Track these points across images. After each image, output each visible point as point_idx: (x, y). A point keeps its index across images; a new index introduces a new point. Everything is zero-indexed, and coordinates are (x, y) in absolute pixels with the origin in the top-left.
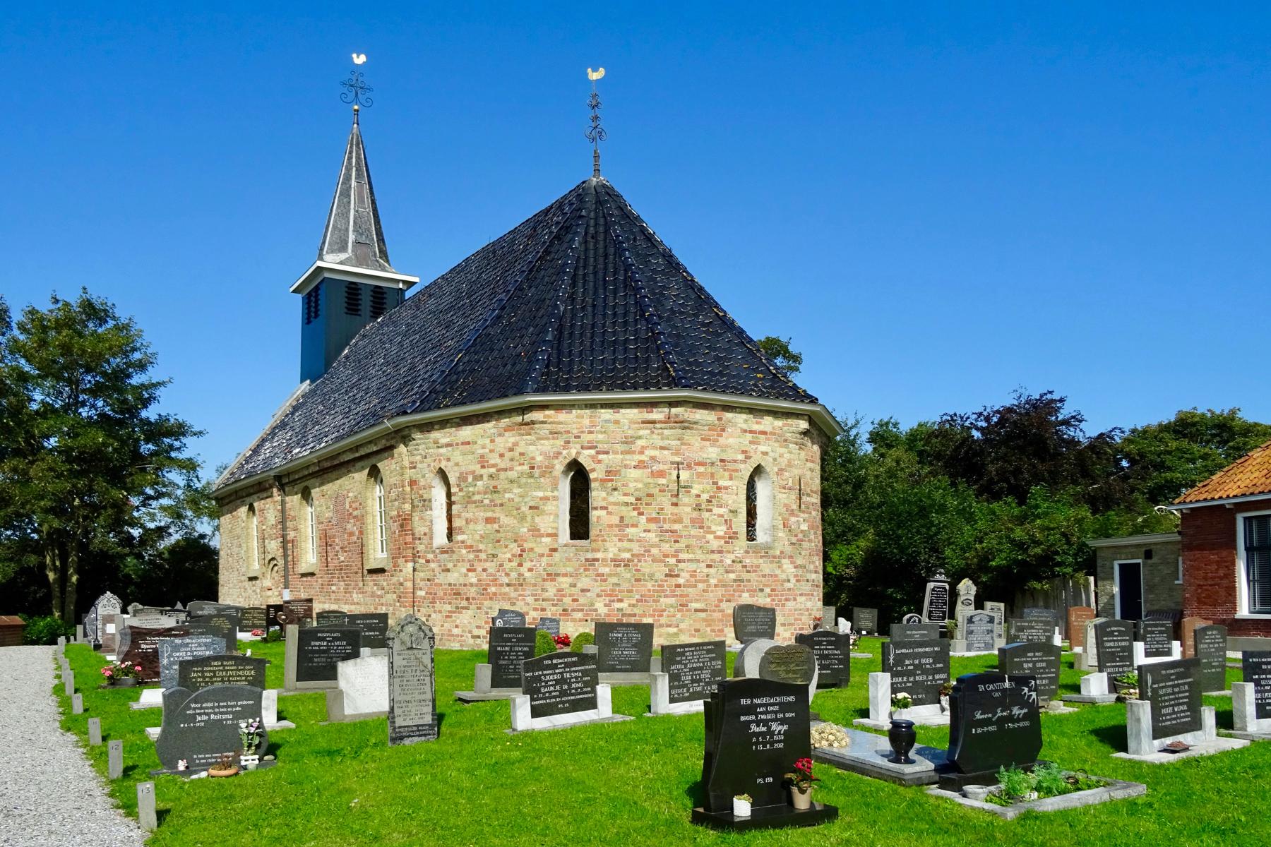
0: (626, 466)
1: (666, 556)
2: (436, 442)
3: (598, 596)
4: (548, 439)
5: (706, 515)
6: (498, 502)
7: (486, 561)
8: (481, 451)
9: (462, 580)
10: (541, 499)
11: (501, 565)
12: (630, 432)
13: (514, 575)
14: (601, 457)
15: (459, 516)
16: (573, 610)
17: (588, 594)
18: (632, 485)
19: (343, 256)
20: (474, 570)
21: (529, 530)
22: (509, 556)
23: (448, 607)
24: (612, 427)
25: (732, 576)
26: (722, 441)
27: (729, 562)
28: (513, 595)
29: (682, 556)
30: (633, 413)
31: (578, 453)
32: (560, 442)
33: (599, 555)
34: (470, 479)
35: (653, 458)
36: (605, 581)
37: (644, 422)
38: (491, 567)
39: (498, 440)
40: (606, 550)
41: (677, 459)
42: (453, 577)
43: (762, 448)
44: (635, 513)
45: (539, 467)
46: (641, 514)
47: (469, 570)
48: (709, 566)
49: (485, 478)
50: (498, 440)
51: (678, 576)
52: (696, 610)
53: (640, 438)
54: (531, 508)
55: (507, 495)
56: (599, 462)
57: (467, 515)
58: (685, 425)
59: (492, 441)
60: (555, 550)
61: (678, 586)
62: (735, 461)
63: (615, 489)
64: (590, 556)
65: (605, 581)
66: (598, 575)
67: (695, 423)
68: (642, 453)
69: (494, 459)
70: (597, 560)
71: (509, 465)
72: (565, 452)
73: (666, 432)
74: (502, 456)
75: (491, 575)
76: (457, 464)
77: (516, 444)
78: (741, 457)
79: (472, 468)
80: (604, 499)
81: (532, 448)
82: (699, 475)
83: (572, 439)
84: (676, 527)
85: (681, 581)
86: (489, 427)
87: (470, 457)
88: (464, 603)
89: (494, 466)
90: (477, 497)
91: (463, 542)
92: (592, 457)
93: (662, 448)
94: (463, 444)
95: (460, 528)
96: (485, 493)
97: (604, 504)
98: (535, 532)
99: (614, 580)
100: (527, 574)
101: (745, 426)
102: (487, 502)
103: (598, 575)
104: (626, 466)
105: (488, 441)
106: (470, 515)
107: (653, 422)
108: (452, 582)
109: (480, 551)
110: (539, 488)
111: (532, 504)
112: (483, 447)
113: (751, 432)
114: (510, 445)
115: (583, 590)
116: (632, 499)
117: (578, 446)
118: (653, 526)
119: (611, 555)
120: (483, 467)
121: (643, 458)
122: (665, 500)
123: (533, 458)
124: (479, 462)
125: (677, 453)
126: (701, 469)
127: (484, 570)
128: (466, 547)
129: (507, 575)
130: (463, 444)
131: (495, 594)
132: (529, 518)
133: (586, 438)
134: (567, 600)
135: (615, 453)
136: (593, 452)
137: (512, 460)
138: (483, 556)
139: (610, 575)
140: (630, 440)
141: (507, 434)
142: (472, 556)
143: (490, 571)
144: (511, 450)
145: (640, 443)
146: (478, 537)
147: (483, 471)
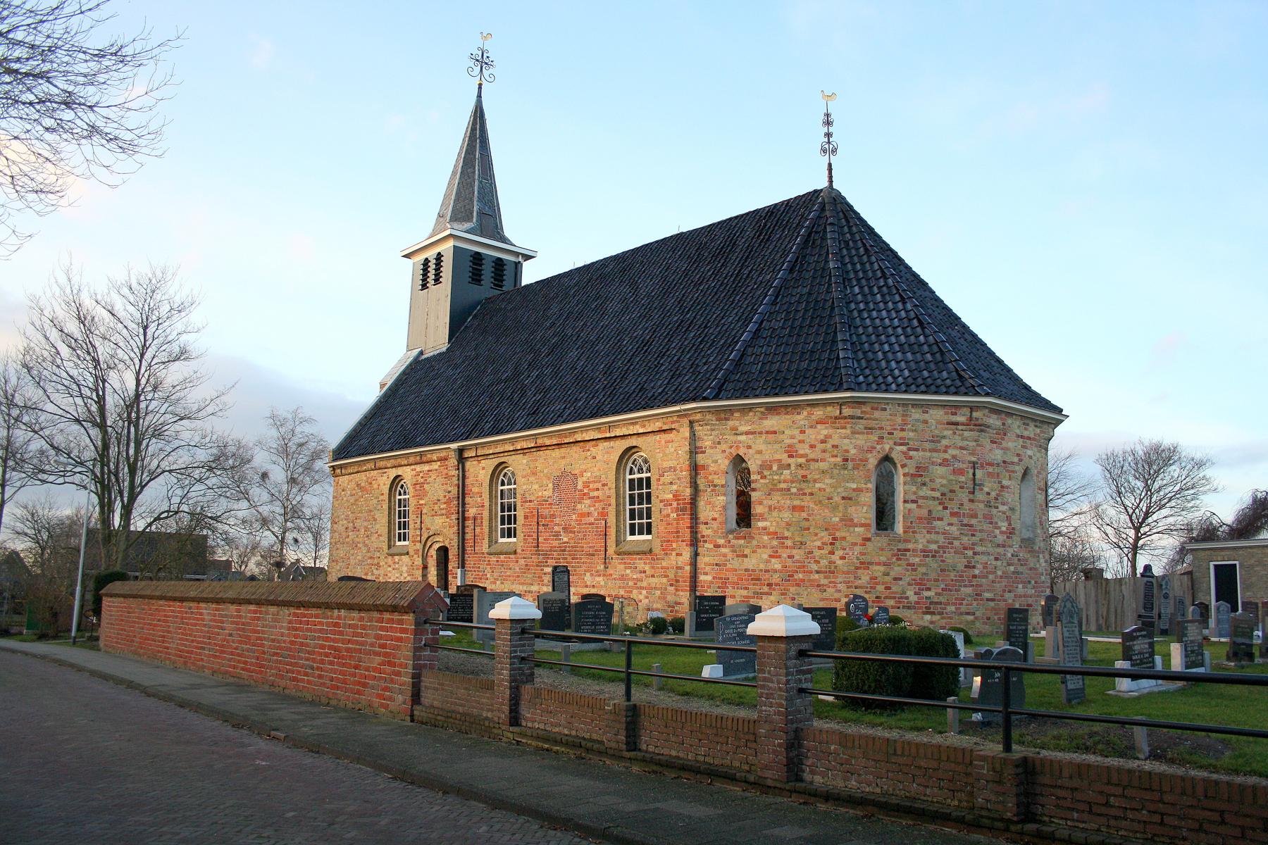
0: (933, 463)
1: (965, 548)
3: (909, 584)
5: (994, 511)
6: (808, 491)
8: (788, 441)
9: (762, 566)
10: (854, 490)
12: (937, 432)
13: (824, 562)
14: (911, 453)
15: (761, 503)
16: (886, 597)
18: (938, 481)
19: (468, 225)
20: (779, 557)
21: (841, 520)
22: (818, 543)
23: (745, 593)
24: (921, 426)
25: (1012, 568)
26: (1004, 444)
27: (1009, 555)
28: (824, 581)
29: (978, 549)
30: (937, 415)
31: (891, 449)
32: (874, 438)
33: (910, 546)
34: (775, 468)
35: (954, 457)
36: (915, 570)
37: (948, 423)
38: (798, 554)
40: (916, 542)
41: (974, 459)
42: (751, 563)
43: (1029, 452)
44: (940, 508)
45: (853, 460)
46: (945, 508)
48: (996, 559)
49: (793, 468)
51: (974, 567)
52: (988, 600)
53: (944, 437)
54: (843, 498)
55: (818, 485)
56: (911, 458)
57: (770, 502)
58: (982, 428)
59: (803, 432)
60: (869, 539)
61: (974, 576)
62: (1013, 463)
63: (924, 484)
64: (901, 546)
65: (915, 570)
66: (909, 565)
68: (945, 451)
70: (908, 550)
71: (820, 457)
73: (966, 434)
74: (812, 447)
75: (798, 561)
76: (760, 452)
77: (828, 436)
78: (1016, 459)
79: (777, 457)
80: (915, 493)
81: (846, 441)
82: (989, 474)
84: (973, 521)
85: (977, 572)
86: (801, 418)
87: (776, 446)
88: (766, 589)
89: (802, 456)
90: (783, 486)
91: (765, 528)
92: (904, 453)
93: (962, 448)
94: (767, 432)
95: (761, 515)
96: (792, 482)
97: (914, 498)
98: (848, 522)
99: (923, 570)
100: (839, 562)
101: (1018, 431)
102: (794, 490)
103: (909, 565)
104: (933, 463)
105: (797, 432)
107: (957, 424)
108: (751, 567)
109: (787, 538)
112: (792, 437)
113: (1022, 437)
114: (822, 437)
115: (895, 579)
116: (937, 494)
117: (891, 442)
118: (955, 520)
119: (920, 546)
121: (947, 456)
122: (964, 496)
123: (847, 451)
124: (786, 452)
125: (972, 454)
126: (991, 470)
127: (790, 557)
128: (769, 534)
130: (767, 432)
131: (803, 580)
132: (841, 508)
133: (898, 434)
134: (880, 588)
135: (924, 450)
136: (904, 448)
137: (824, 451)
138: (789, 543)
139: (920, 565)
140: (936, 440)
141: (819, 426)
142: (775, 543)
143: (797, 557)
144: (823, 442)
145: (944, 442)
146: (784, 525)
147: (791, 461)
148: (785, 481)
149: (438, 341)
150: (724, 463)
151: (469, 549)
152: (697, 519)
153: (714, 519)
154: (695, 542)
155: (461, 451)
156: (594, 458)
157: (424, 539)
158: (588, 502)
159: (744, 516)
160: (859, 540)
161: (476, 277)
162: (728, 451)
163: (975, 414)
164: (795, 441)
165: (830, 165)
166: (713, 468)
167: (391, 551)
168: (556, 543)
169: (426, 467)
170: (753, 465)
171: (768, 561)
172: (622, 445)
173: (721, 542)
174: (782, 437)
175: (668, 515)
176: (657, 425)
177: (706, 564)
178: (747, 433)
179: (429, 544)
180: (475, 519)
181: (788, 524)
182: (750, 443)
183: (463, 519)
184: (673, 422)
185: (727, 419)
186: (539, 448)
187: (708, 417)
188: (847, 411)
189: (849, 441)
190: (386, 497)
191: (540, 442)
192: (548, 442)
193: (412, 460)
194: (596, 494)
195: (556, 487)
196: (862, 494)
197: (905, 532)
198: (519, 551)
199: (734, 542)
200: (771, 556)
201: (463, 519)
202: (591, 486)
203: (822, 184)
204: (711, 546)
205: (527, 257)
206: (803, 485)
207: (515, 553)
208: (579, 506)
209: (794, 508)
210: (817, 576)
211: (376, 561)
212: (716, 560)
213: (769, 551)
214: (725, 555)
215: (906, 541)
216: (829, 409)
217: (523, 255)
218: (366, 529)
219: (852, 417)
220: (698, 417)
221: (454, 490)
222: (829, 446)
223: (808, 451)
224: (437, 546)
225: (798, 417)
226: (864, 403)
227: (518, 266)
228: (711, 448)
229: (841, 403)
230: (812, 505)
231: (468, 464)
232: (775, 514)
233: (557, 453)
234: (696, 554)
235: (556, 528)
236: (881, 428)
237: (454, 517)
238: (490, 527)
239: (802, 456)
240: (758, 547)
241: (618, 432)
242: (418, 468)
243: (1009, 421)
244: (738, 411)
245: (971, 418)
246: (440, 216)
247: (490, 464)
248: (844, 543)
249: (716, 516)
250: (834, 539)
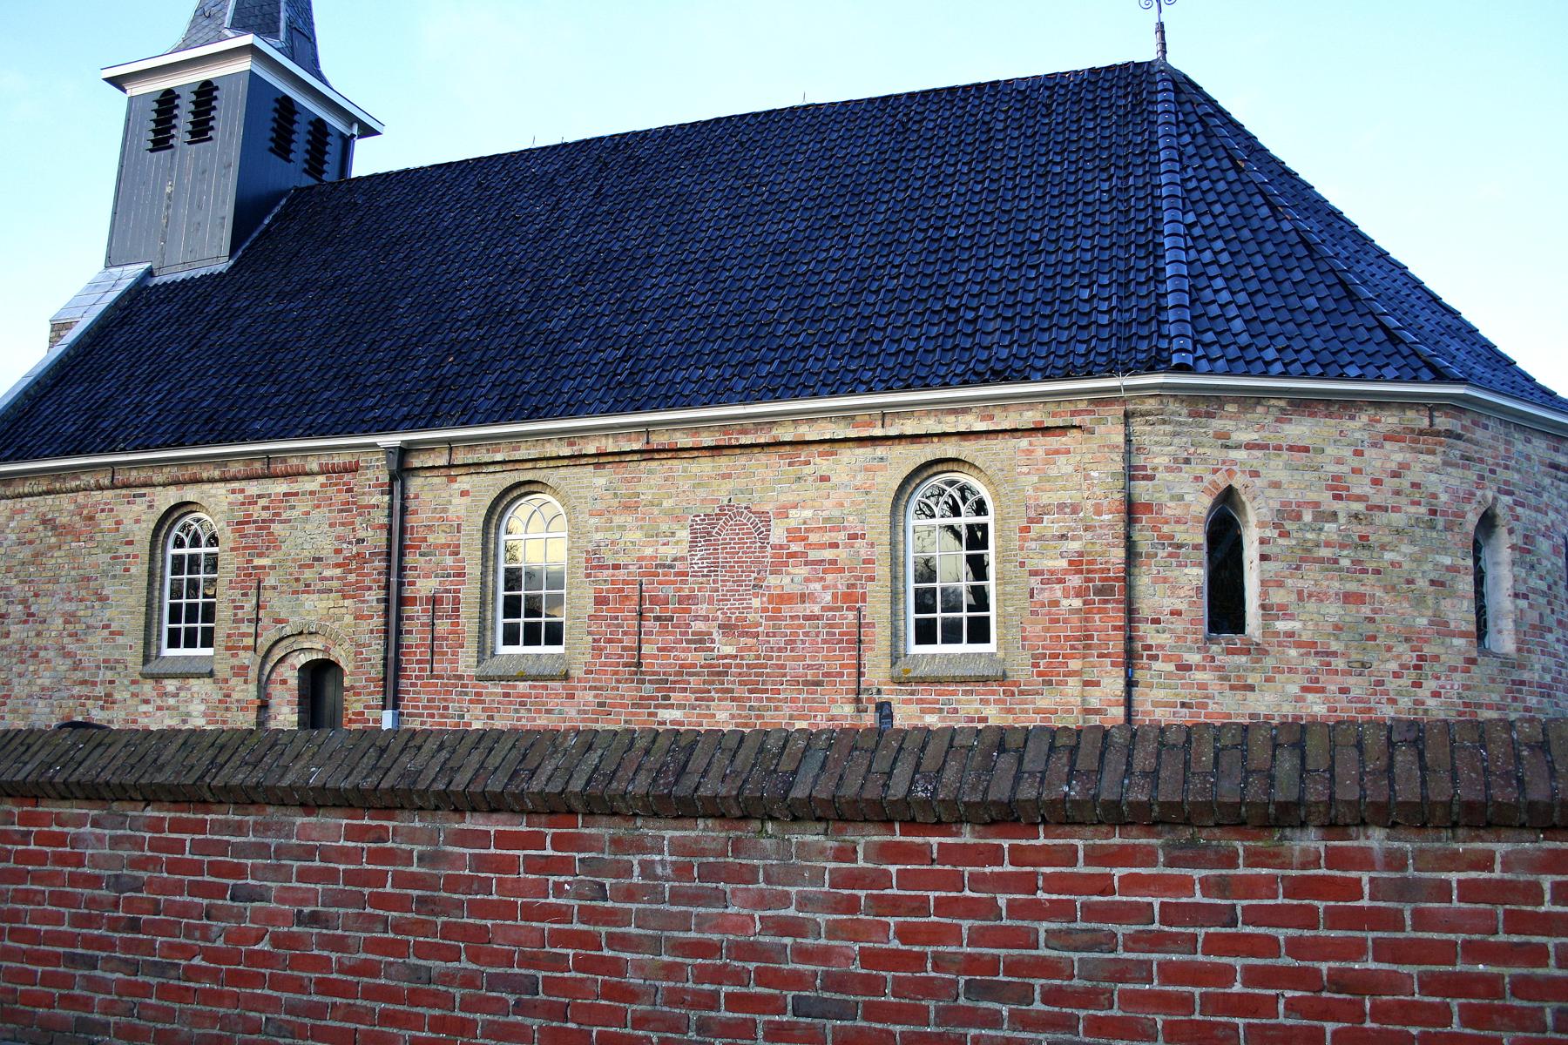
2: (1222, 436)
4: (1456, 465)
6: (1370, 566)
7: (1345, 673)
8: (1333, 469)
10: (1449, 569)
11: (1380, 683)
14: (1519, 510)
20: (1322, 690)
21: (1431, 623)
22: (1393, 666)
32: (1472, 476)
33: (1526, 676)
34: (1308, 517)
39: (1370, 453)
45: (1444, 513)
47: (1305, 689)
49: (1342, 519)
50: (1370, 453)
54: (1433, 583)
55: (1388, 556)
57: (1300, 584)
69: (1361, 486)
70: (1522, 683)
71: (1391, 501)
72: (1479, 493)
74: (1376, 482)
75: (1360, 700)
76: (1276, 485)
77: (1404, 466)
79: (1312, 496)
81: (1434, 477)
83: (1487, 474)
86: (1357, 426)
87: (1308, 476)
89: (1359, 498)
90: (1325, 552)
91: (1291, 634)
94: (1291, 448)
96: (1343, 546)
98: (1440, 625)
100: (1431, 703)
102: (1345, 563)
105: (1347, 452)
106: (1307, 585)
109: (1334, 654)
110: (1444, 550)
111: (1433, 575)
114: (1394, 466)
120: (1337, 497)
123: (1434, 496)
127: (1344, 691)
128: (1299, 645)
129: (1393, 701)
130: (1291, 448)
132: (1430, 601)
137: (1397, 493)
138: (1339, 663)
141: (1388, 445)
142: (1313, 662)
143: (1356, 692)
144: (1395, 475)
146: (1330, 629)
147: (1338, 506)
148: (1328, 544)
149: (202, 248)
150: (1202, 504)
151: (412, 668)
153: (1176, 613)
154: (1130, 659)
155: (404, 451)
156: (824, 479)
157: (264, 642)
158: (804, 571)
159: (1225, 609)
160: (1460, 664)
161: (282, 146)
162: (1208, 477)
165: (1161, 29)
166: (1172, 509)
167: (153, 667)
168: (698, 658)
169: (281, 487)
171: (1298, 699)
173: (1194, 658)
174: (1320, 458)
175: (1056, 603)
176: (1029, 418)
177: (1156, 704)
178: (1250, 446)
179: (277, 654)
180: (434, 601)
181: (1337, 627)
182: (1256, 465)
183: (396, 603)
184: (1074, 413)
185: (1210, 415)
186: (648, 453)
187: (1173, 406)
188: (1443, 422)
189: (1440, 479)
190: (143, 549)
191: (658, 440)
192: (684, 441)
193: (235, 468)
194: (828, 554)
195: (702, 535)
196: (1460, 576)
197: (1519, 650)
198: (577, 672)
199: (1222, 659)
200: (1305, 689)
201: (396, 603)
202: (814, 538)
203: (1145, 52)
204: (1171, 667)
205: (368, 131)
206: (1363, 555)
207: (566, 677)
208: (772, 580)
209: (1348, 598)
211: (100, 690)
212: (1185, 695)
213: (1303, 680)
214: (1203, 686)
215: (1522, 667)
216: (1410, 414)
218: (70, 618)
219: (1449, 434)
220: (1151, 404)
221: (376, 539)
223: (1368, 490)
224: (303, 659)
225: (1352, 424)
227: (347, 144)
228: (1168, 469)
229: (1433, 405)
230: (1379, 593)
231: (415, 484)
232: (1311, 606)
233: (705, 466)
235: (698, 626)
236: (1481, 461)
237: (374, 596)
239: (1359, 498)
240: (1277, 670)
241: (910, 427)
242: (253, 488)
244: (1235, 400)
248: (1437, 667)
249: (1183, 606)
250: (1420, 658)
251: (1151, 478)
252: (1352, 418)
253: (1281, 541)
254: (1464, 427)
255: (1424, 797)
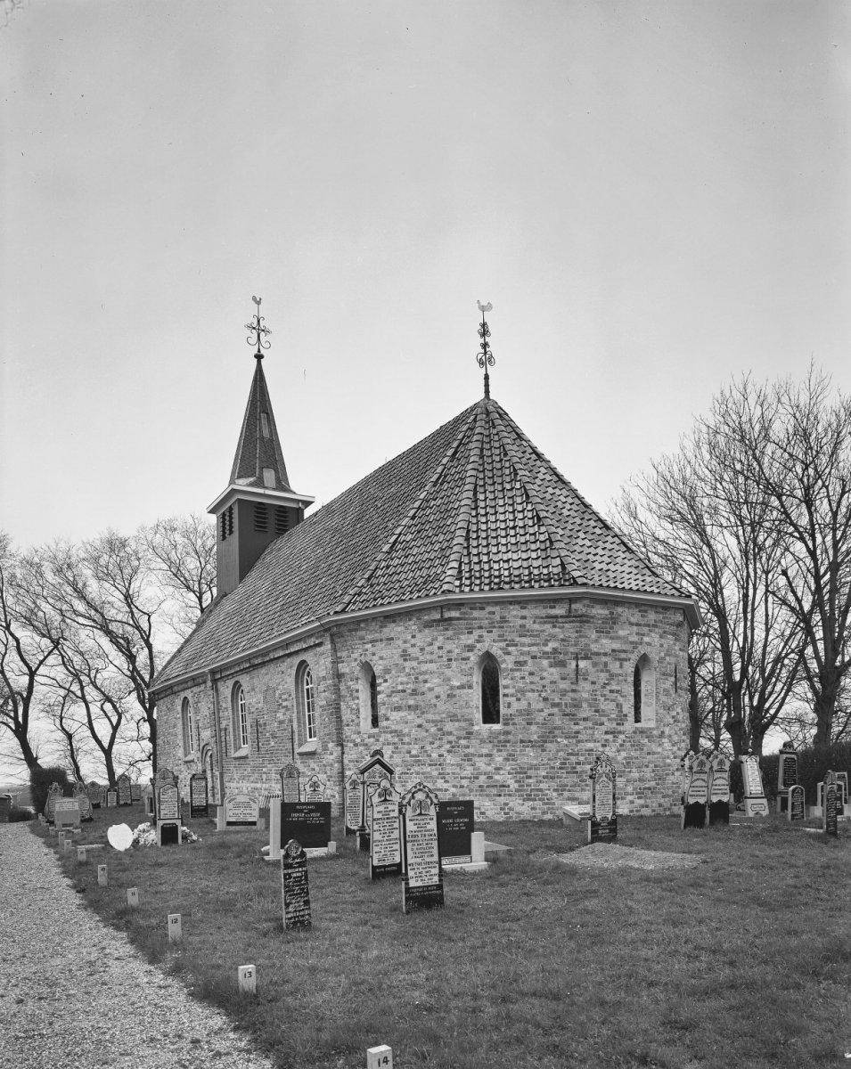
8: (403, 646)
14: (510, 649)
17: (502, 772)
37: (547, 617)
58: (583, 619)
59: (414, 637)
67: (592, 617)
72: (478, 645)
75: (416, 756)
83: (485, 634)
107: (556, 617)
120: (405, 660)
124: (402, 656)
134: (483, 778)
143: (414, 752)
152: (341, 721)
162: (359, 659)
163: (573, 606)
164: (409, 645)
170: (378, 670)
172: (296, 660)
179: (205, 752)
185: (356, 630)
186: (255, 667)
204: (352, 745)
210: (429, 769)
217: (303, 502)
222: (435, 647)
223: (419, 654)
226: (462, 605)
234: (343, 753)
236: (480, 628)
238: (235, 736)
243: (620, 610)
245: (570, 611)
246: (233, 473)
247: (230, 683)
251: (343, 662)
252: (410, 620)
253: (385, 684)
254: (461, 614)
255: (746, 798)
